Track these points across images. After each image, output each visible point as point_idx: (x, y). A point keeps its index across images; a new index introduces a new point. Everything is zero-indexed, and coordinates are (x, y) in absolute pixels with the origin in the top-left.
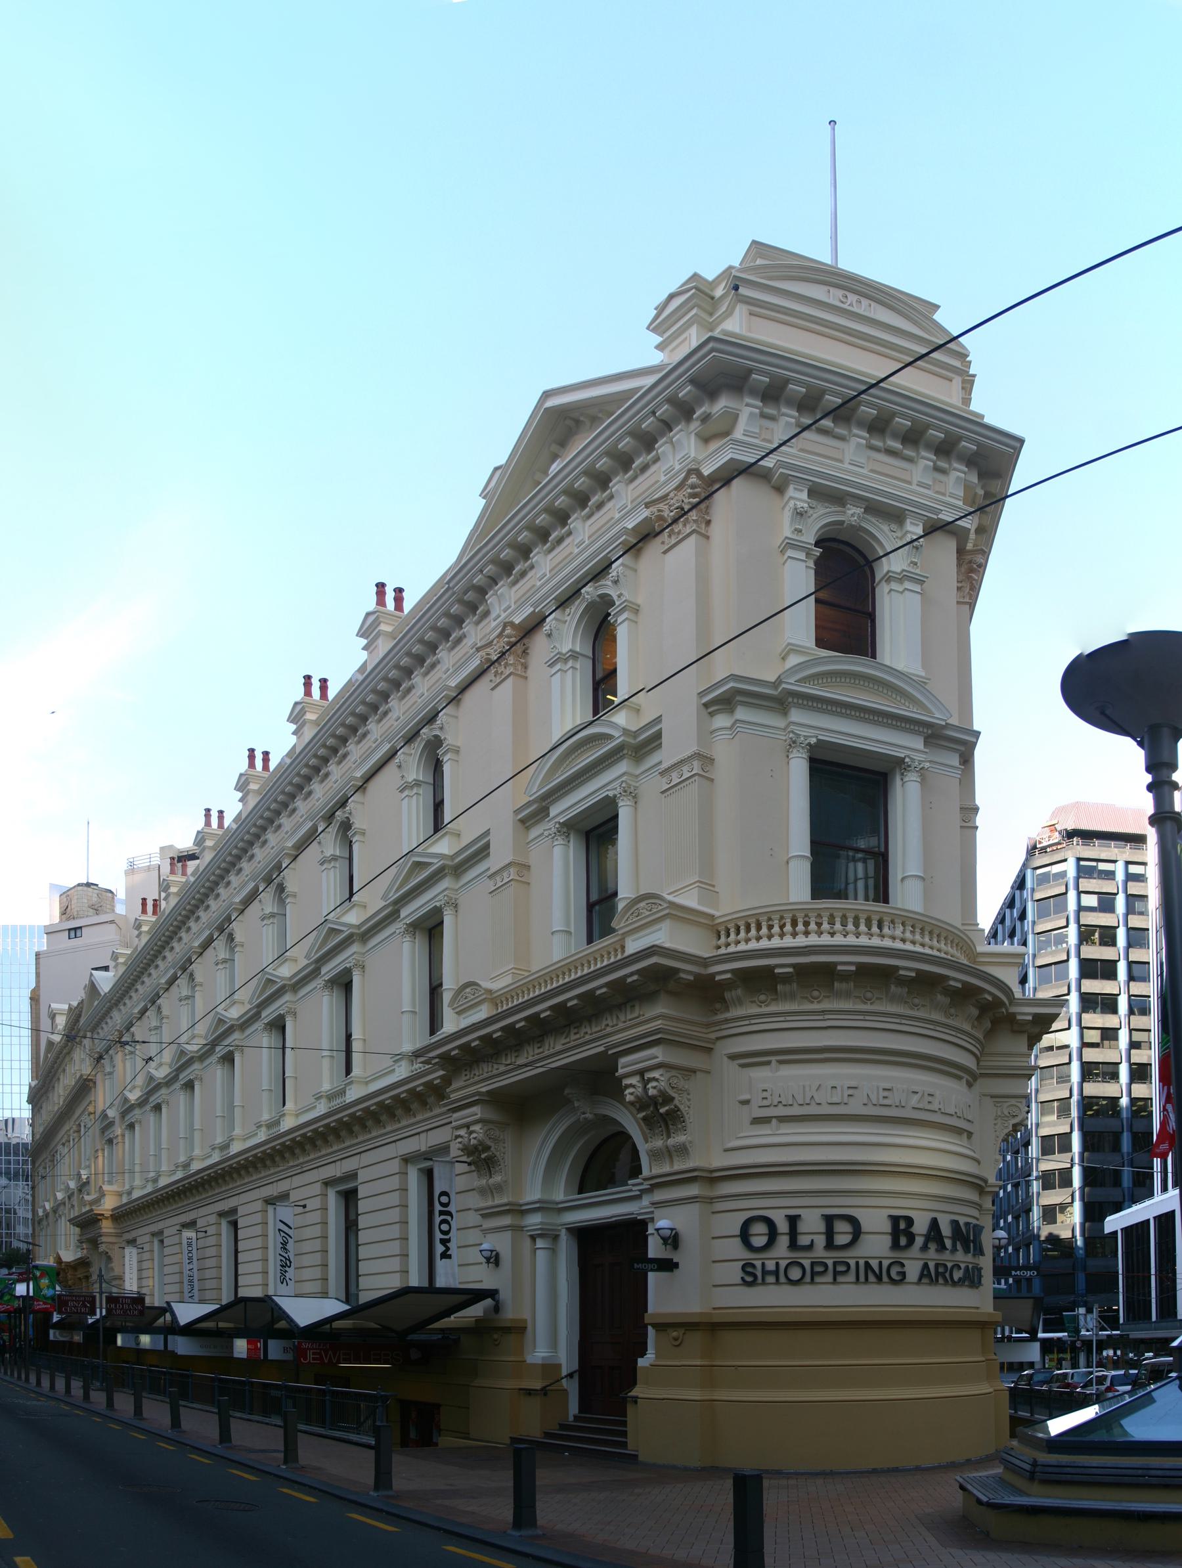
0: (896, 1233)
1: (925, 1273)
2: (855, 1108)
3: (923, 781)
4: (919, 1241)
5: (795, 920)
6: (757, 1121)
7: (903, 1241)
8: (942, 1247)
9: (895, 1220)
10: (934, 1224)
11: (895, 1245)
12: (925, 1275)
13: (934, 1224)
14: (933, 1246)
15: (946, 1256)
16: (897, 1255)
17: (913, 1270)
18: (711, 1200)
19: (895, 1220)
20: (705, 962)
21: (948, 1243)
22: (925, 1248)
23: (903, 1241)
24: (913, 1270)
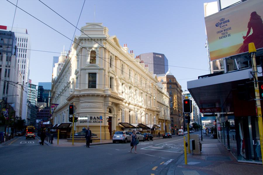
0: (91, 118)
1: (93, 122)
2: (88, 107)
3: (99, 74)
4: (93, 119)
5: (86, 90)
6: (82, 108)
7: (91, 119)
8: (96, 119)
9: (91, 117)
10: (95, 117)
11: (91, 119)
12: (93, 122)
13: (95, 117)
14: (94, 119)
15: (95, 120)
16: (91, 120)
17: (92, 121)
18: (79, 115)
19: (91, 117)
20: (77, 95)
21: (96, 119)
22: (94, 119)
23: (91, 119)
24: (92, 121)
